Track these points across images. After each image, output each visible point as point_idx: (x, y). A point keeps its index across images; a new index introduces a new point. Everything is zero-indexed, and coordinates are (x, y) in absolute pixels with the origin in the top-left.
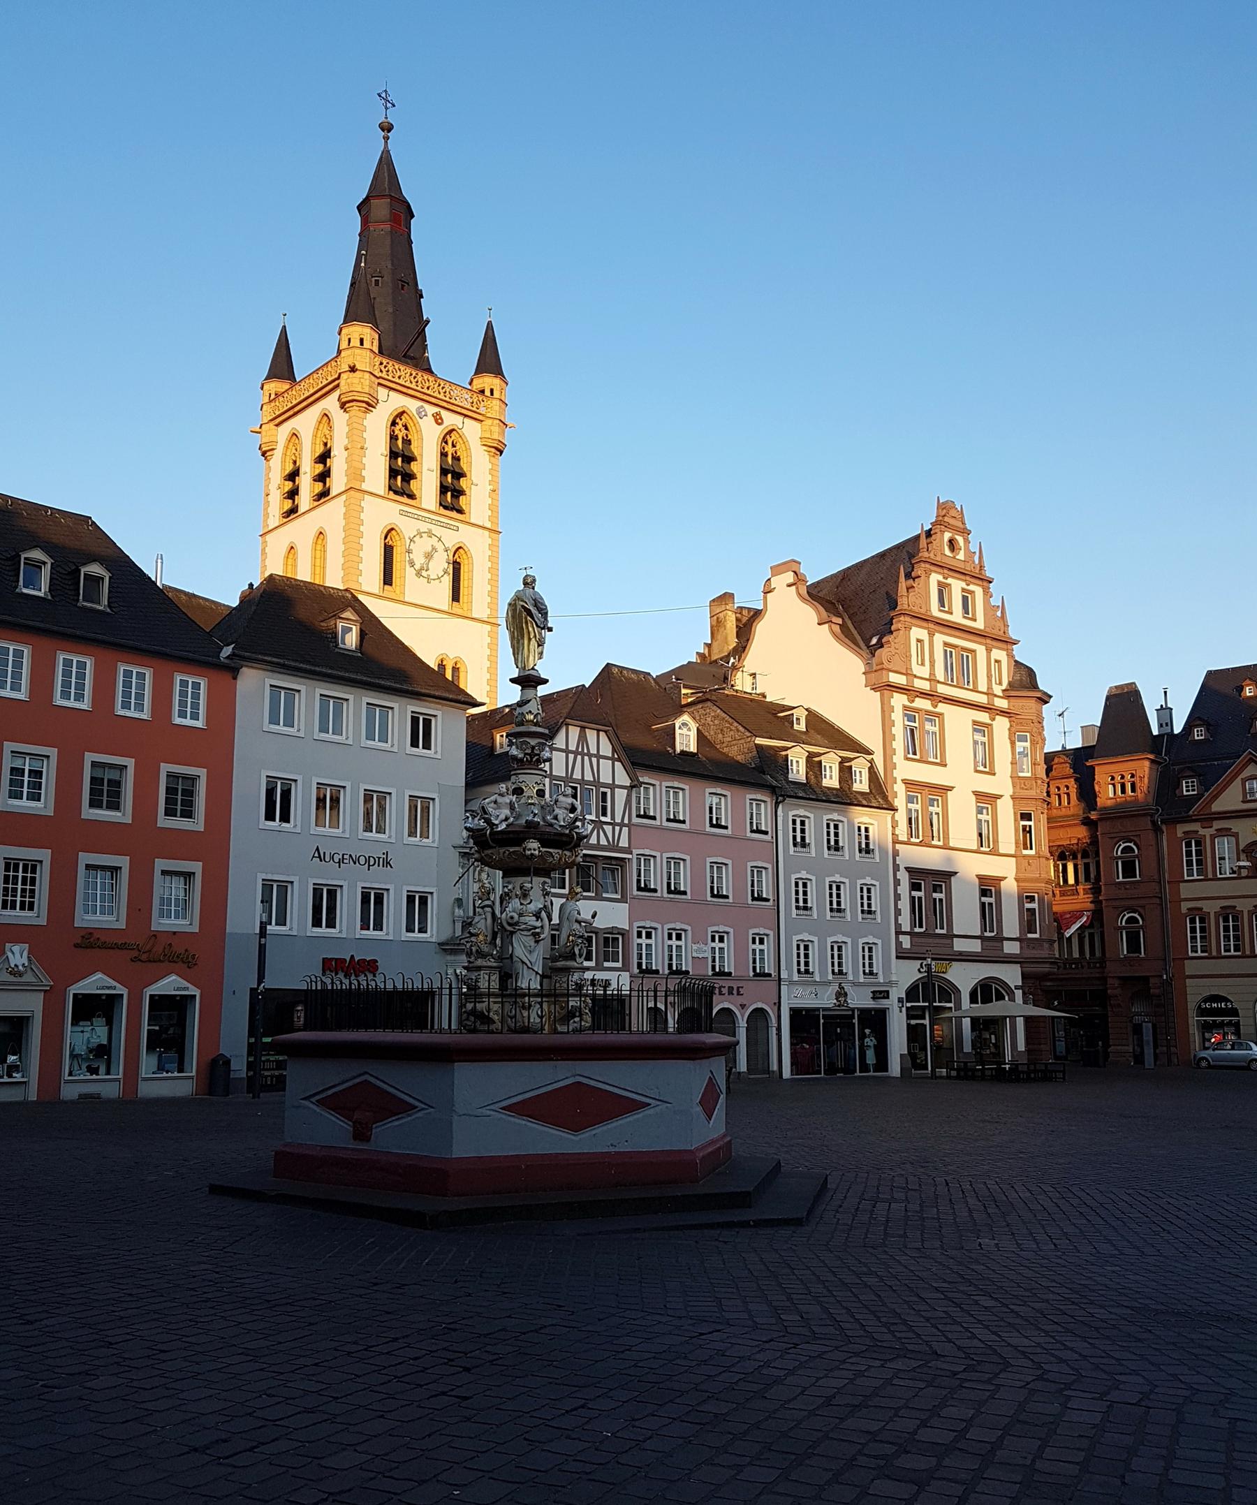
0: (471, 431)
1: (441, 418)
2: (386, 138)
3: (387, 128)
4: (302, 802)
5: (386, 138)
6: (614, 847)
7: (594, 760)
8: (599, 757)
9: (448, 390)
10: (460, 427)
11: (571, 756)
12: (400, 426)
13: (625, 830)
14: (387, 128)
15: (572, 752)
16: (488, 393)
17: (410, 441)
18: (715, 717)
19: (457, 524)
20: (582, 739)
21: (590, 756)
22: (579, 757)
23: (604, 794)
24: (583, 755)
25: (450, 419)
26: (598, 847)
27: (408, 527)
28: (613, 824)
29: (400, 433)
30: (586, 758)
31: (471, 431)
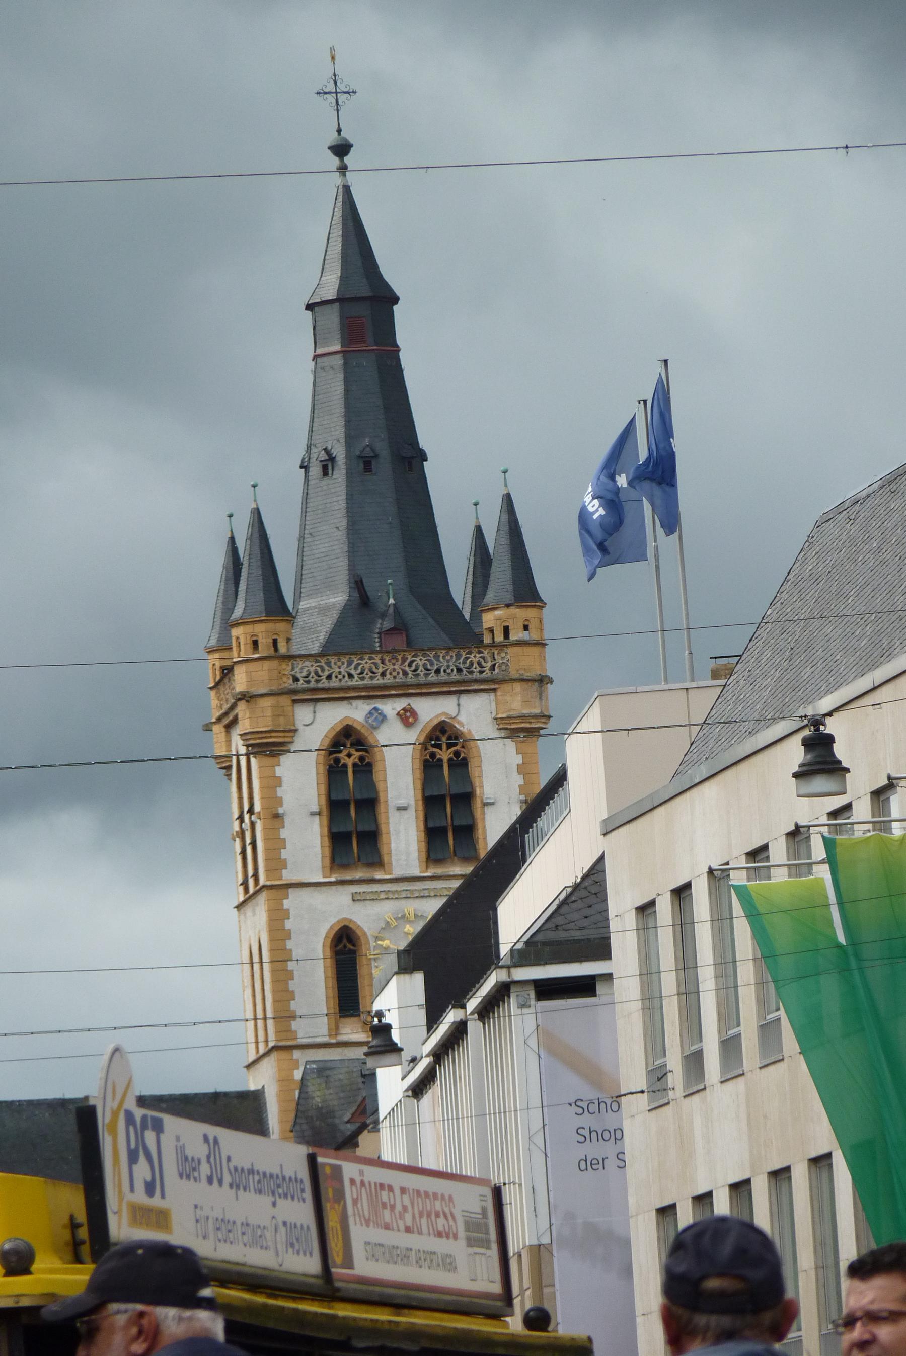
1: (414, 714)
2: (343, 169)
3: (341, 150)
5: (343, 169)
9: (421, 663)
14: (341, 150)
17: (370, 765)
29: (349, 758)
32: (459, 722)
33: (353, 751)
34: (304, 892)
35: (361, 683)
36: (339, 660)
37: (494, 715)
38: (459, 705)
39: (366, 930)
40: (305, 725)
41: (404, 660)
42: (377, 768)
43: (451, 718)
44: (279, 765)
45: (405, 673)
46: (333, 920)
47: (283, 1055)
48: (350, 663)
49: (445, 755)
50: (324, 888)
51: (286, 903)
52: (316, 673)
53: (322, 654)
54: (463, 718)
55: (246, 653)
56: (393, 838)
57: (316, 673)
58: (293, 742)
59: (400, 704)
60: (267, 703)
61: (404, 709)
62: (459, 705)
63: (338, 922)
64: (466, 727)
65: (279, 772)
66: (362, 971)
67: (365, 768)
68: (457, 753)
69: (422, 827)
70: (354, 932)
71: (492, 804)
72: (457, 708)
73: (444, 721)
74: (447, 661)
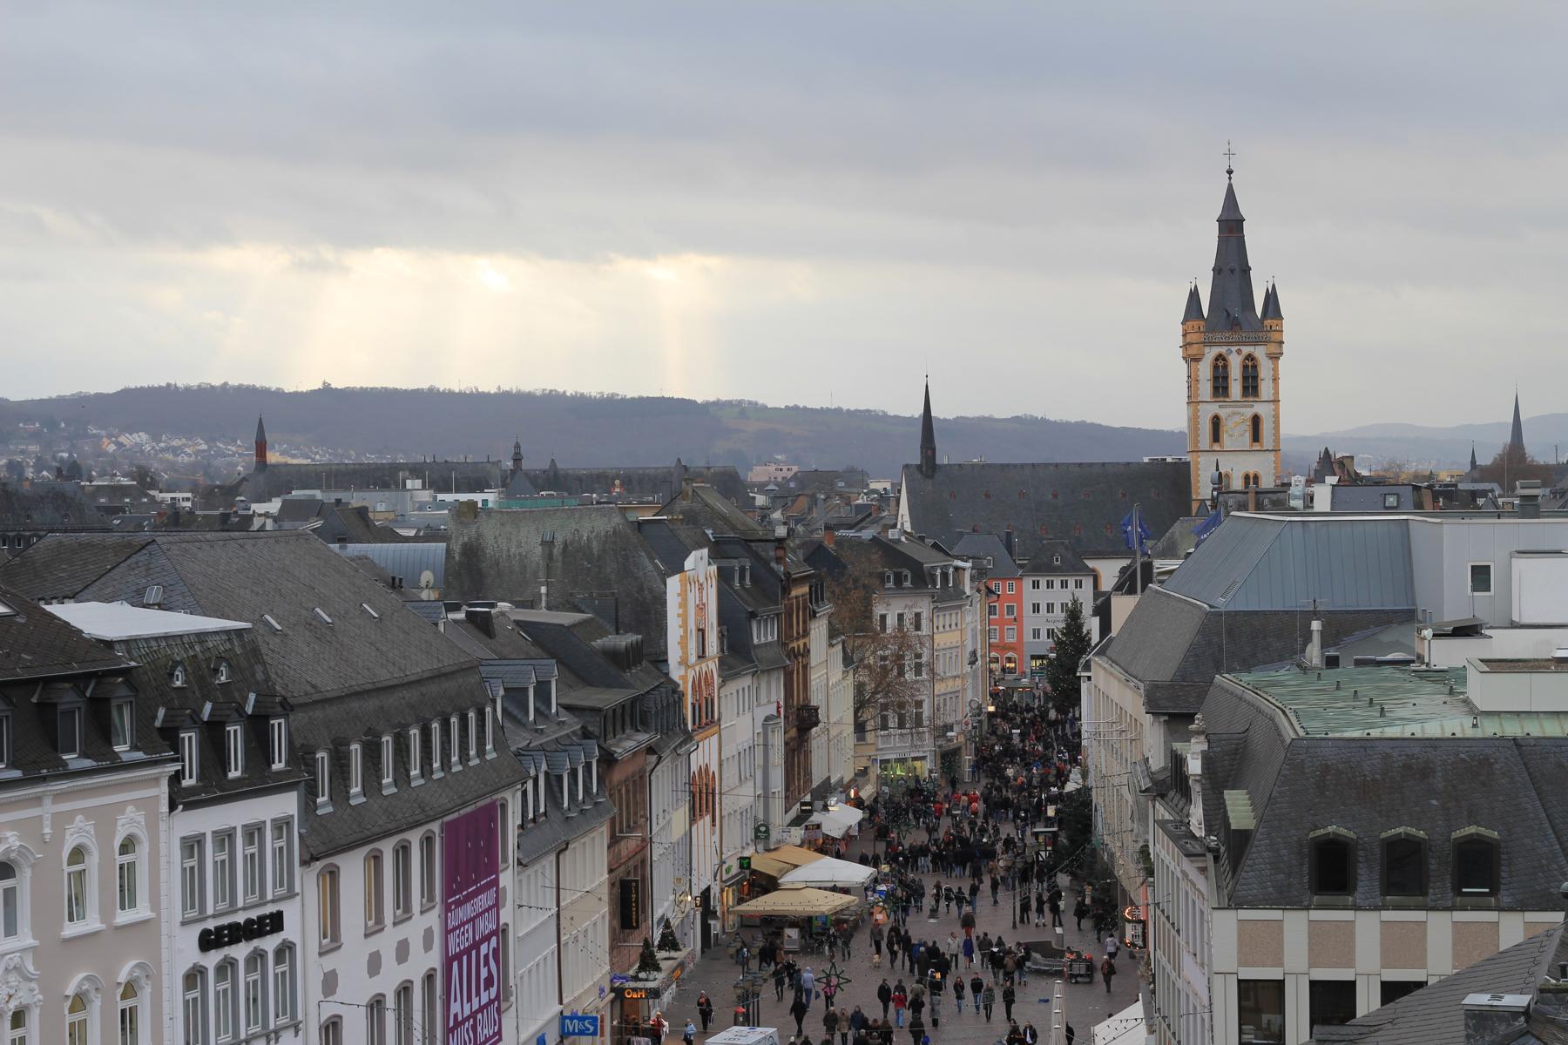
0: (1260, 352)
2: (1230, 178)
3: (1230, 172)
4: (1043, 608)
5: (1230, 178)
14: (1230, 172)
25: (1246, 350)
27: (1223, 413)
29: (1221, 363)
31: (1260, 352)
42: (1229, 367)
47: (1194, 453)
49: (1250, 364)
59: (1237, 348)
67: (1225, 367)
74: (1252, 335)
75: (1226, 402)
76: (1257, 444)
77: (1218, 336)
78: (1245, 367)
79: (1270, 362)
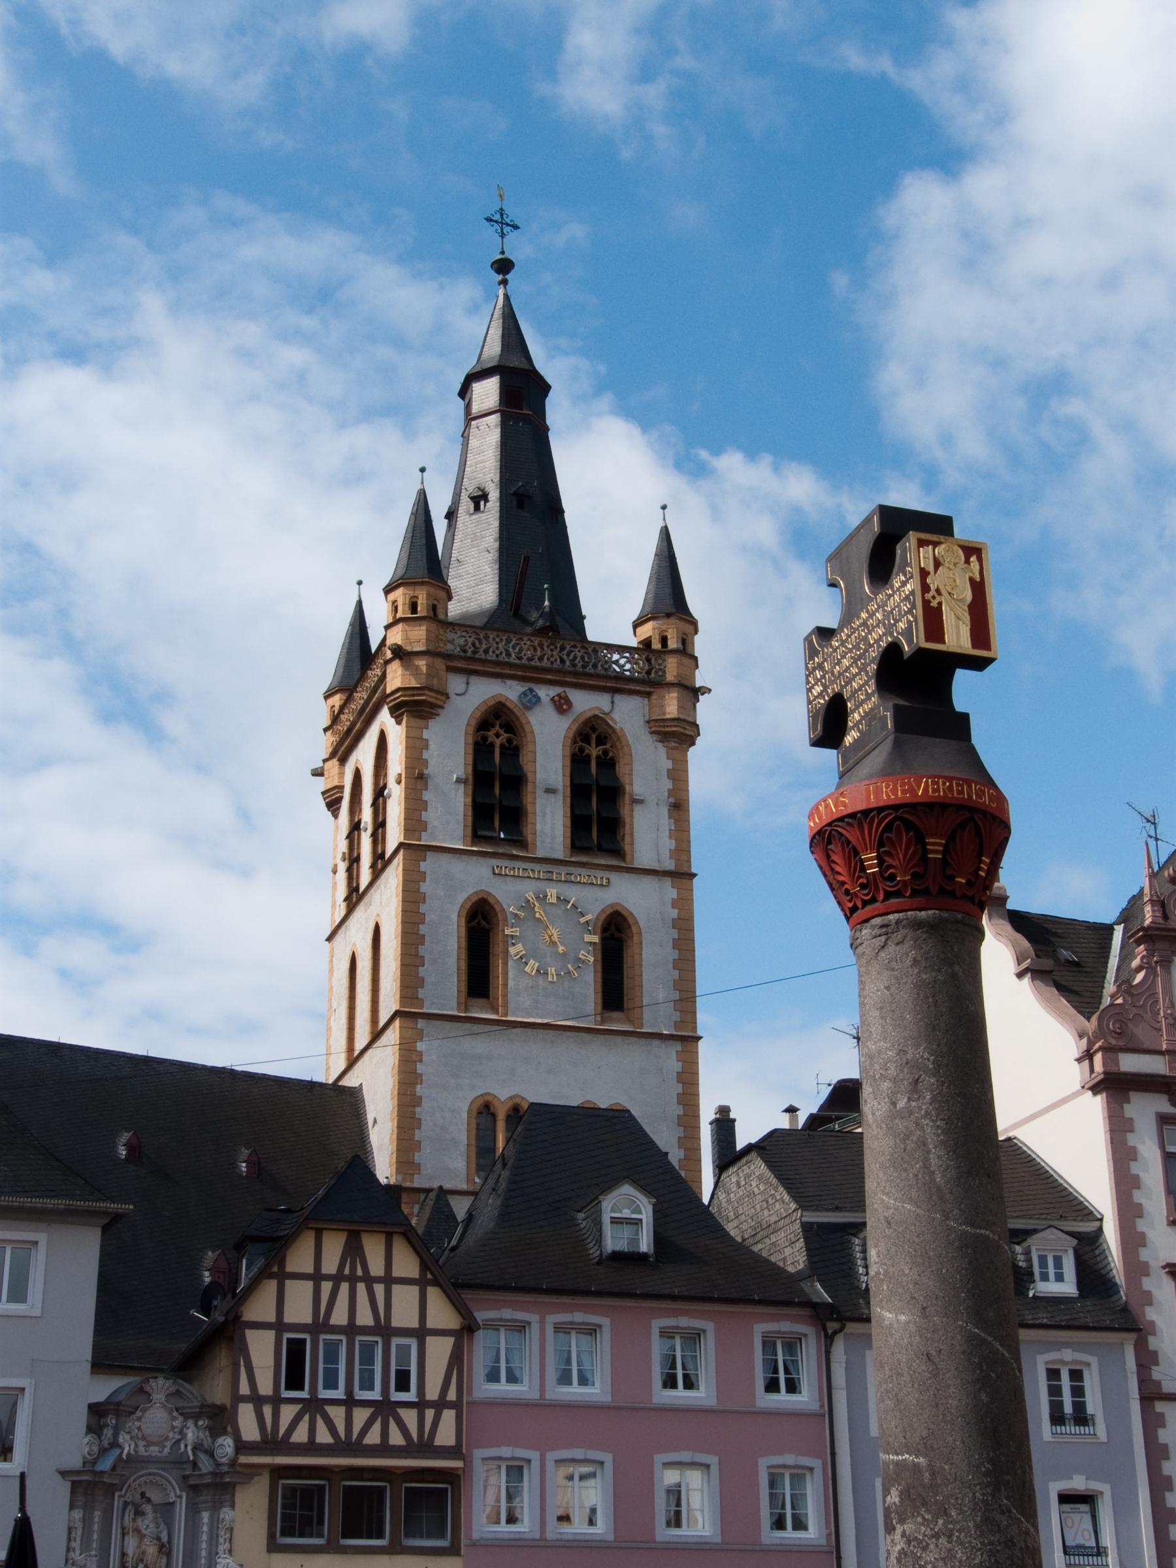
1: (569, 703)
3: (504, 266)
6: (425, 1447)
7: (379, 1289)
8: (389, 1280)
9: (579, 655)
10: (607, 709)
11: (326, 1287)
12: (497, 728)
13: (449, 1416)
14: (504, 266)
15: (328, 1277)
16: (656, 645)
18: (760, 1178)
19: (606, 874)
20: (353, 1250)
21: (369, 1281)
22: (345, 1287)
23: (404, 1351)
24: (353, 1280)
25: (585, 702)
26: (384, 1449)
28: (420, 1405)
30: (361, 1288)
32: (612, 719)
33: (502, 732)
34: (444, 858)
35: (517, 661)
36: (498, 636)
37: (647, 718)
38: (613, 702)
39: (505, 906)
40: (457, 695)
41: (562, 649)
43: (605, 714)
44: (427, 728)
45: (563, 661)
46: (471, 891)
47: (409, 1023)
48: (509, 641)
49: (594, 751)
50: (465, 857)
51: (423, 866)
52: (473, 644)
53: (485, 627)
54: (616, 715)
55: (404, 612)
56: (538, 818)
57: (473, 644)
58: (442, 707)
59: (554, 691)
60: (422, 663)
61: (559, 695)
62: (613, 702)
63: (476, 893)
64: (618, 725)
65: (426, 734)
66: (497, 948)
67: (513, 751)
68: (605, 752)
69: (569, 814)
70: (492, 907)
71: (641, 802)
72: (610, 705)
73: (596, 716)
75: (517, 858)
76: (616, 1015)
77: (498, 646)
78: (578, 761)
79: (662, 750)
